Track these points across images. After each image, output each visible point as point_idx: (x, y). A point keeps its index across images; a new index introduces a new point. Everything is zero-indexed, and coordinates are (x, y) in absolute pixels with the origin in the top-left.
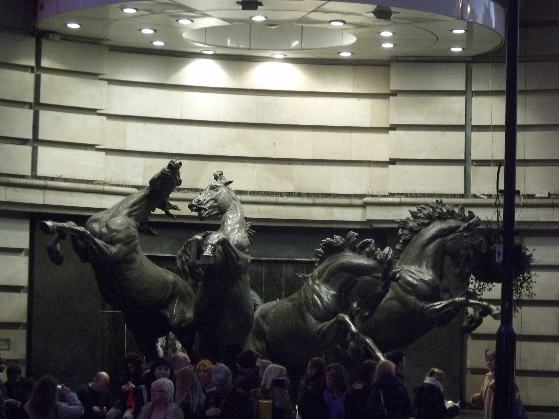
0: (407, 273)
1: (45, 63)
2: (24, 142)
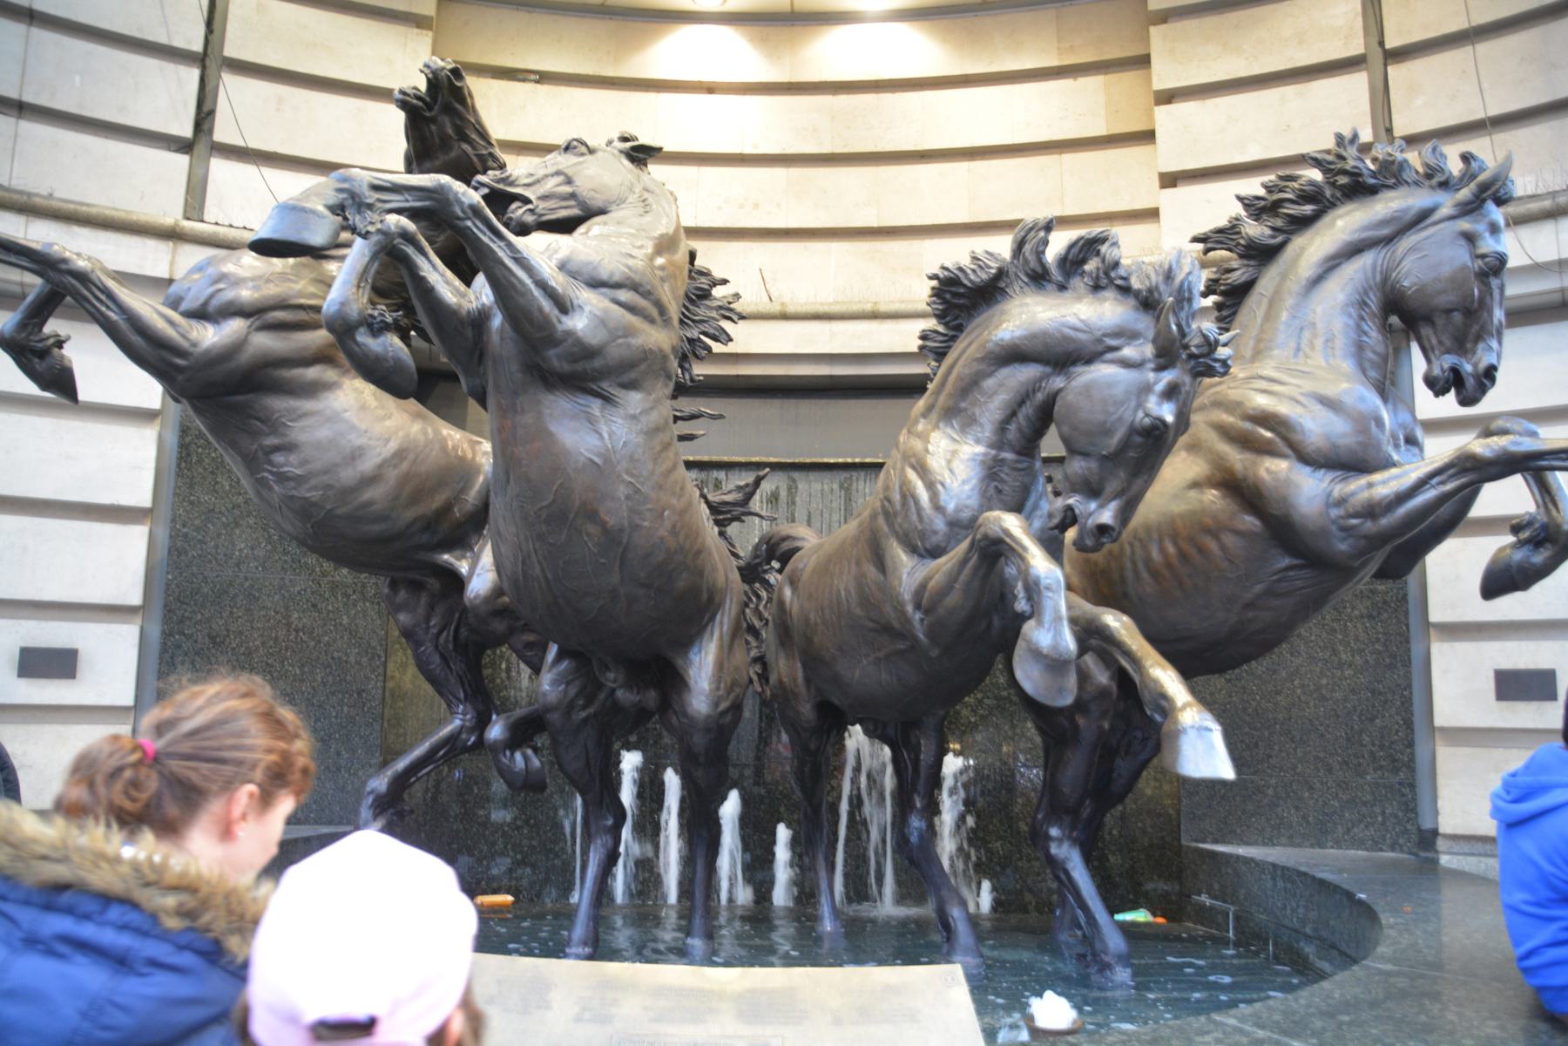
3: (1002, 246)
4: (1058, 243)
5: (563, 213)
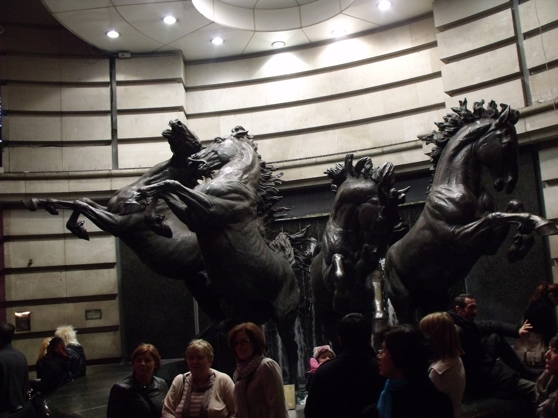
0: (436, 195)
1: (120, 77)
2: (106, 143)
3: (343, 163)
4: (355, 163)
5: (216, 164)
